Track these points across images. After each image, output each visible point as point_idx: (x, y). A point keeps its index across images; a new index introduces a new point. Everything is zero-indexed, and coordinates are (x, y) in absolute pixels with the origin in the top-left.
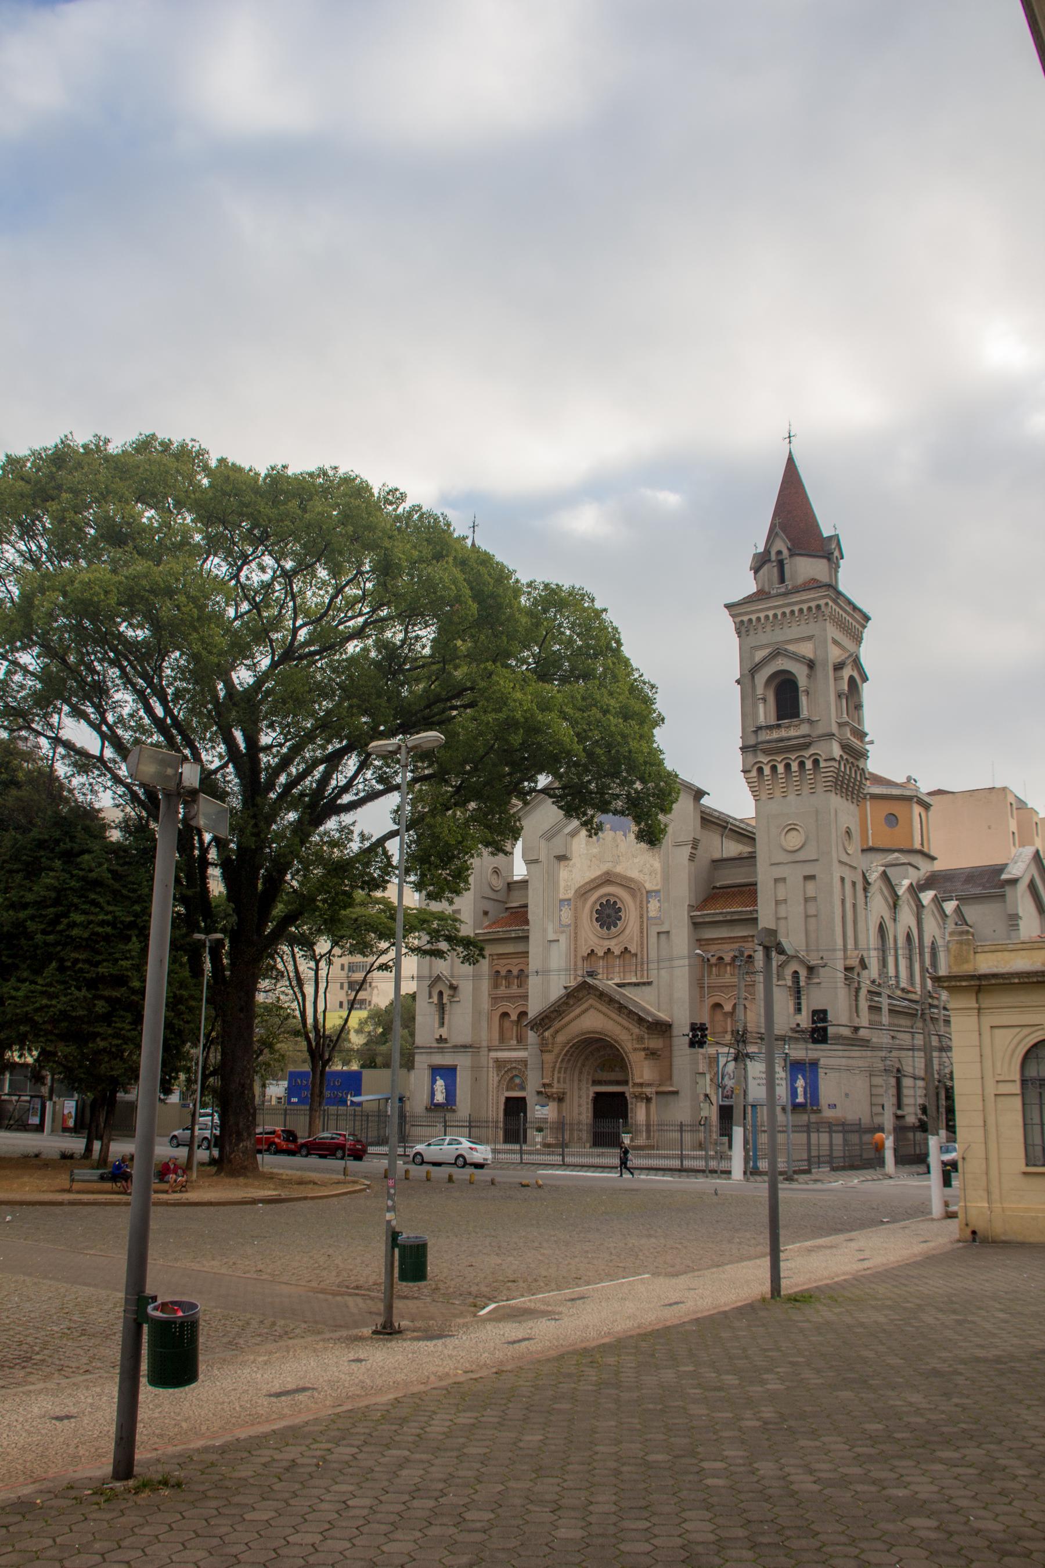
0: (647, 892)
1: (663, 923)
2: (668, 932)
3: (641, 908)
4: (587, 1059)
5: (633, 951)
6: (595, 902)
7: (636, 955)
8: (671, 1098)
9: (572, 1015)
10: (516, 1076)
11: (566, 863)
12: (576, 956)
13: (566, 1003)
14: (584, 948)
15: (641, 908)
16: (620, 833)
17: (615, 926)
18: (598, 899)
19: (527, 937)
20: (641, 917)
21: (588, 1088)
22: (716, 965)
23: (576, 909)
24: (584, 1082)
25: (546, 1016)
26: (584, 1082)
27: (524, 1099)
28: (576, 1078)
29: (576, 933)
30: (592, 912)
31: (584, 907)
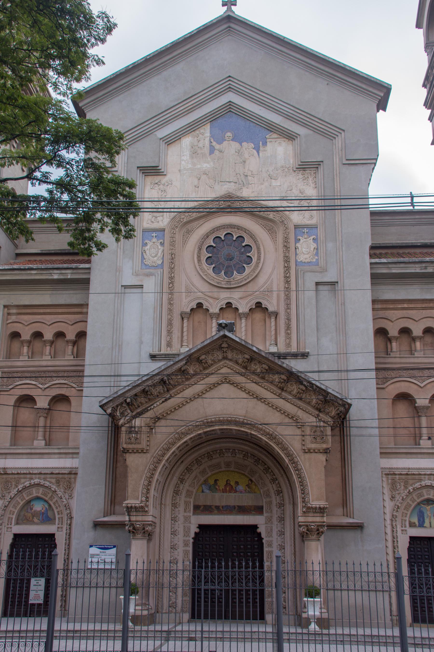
0: (296, 227)
1: (324, 270)
2: (333, 284)
3: (286, 247)
4: (188, 469)
5: (271, 309)
6: (207, 236)
7: (276, 314)
8: (350, 535)
9: (189, 392)
10: (38, 498)
11: (157, 179)
12: (170, 311)
13: (182, 372)
14: (185, 301)
15: (286, 247)
16: (248, 147)
17: (241, 270)
18: (214, 230)
19: (87, 282)
20: (287, 260)
21: (187, 519)
22: (396, 338)
23: (173, 244)
24: (181, 508)
25: (144, 392)
26: (181, 508)
27: (52, 536)
28: (168, 501)
29: (171, 278)
30: (200, 249)
31: (185, 242)
